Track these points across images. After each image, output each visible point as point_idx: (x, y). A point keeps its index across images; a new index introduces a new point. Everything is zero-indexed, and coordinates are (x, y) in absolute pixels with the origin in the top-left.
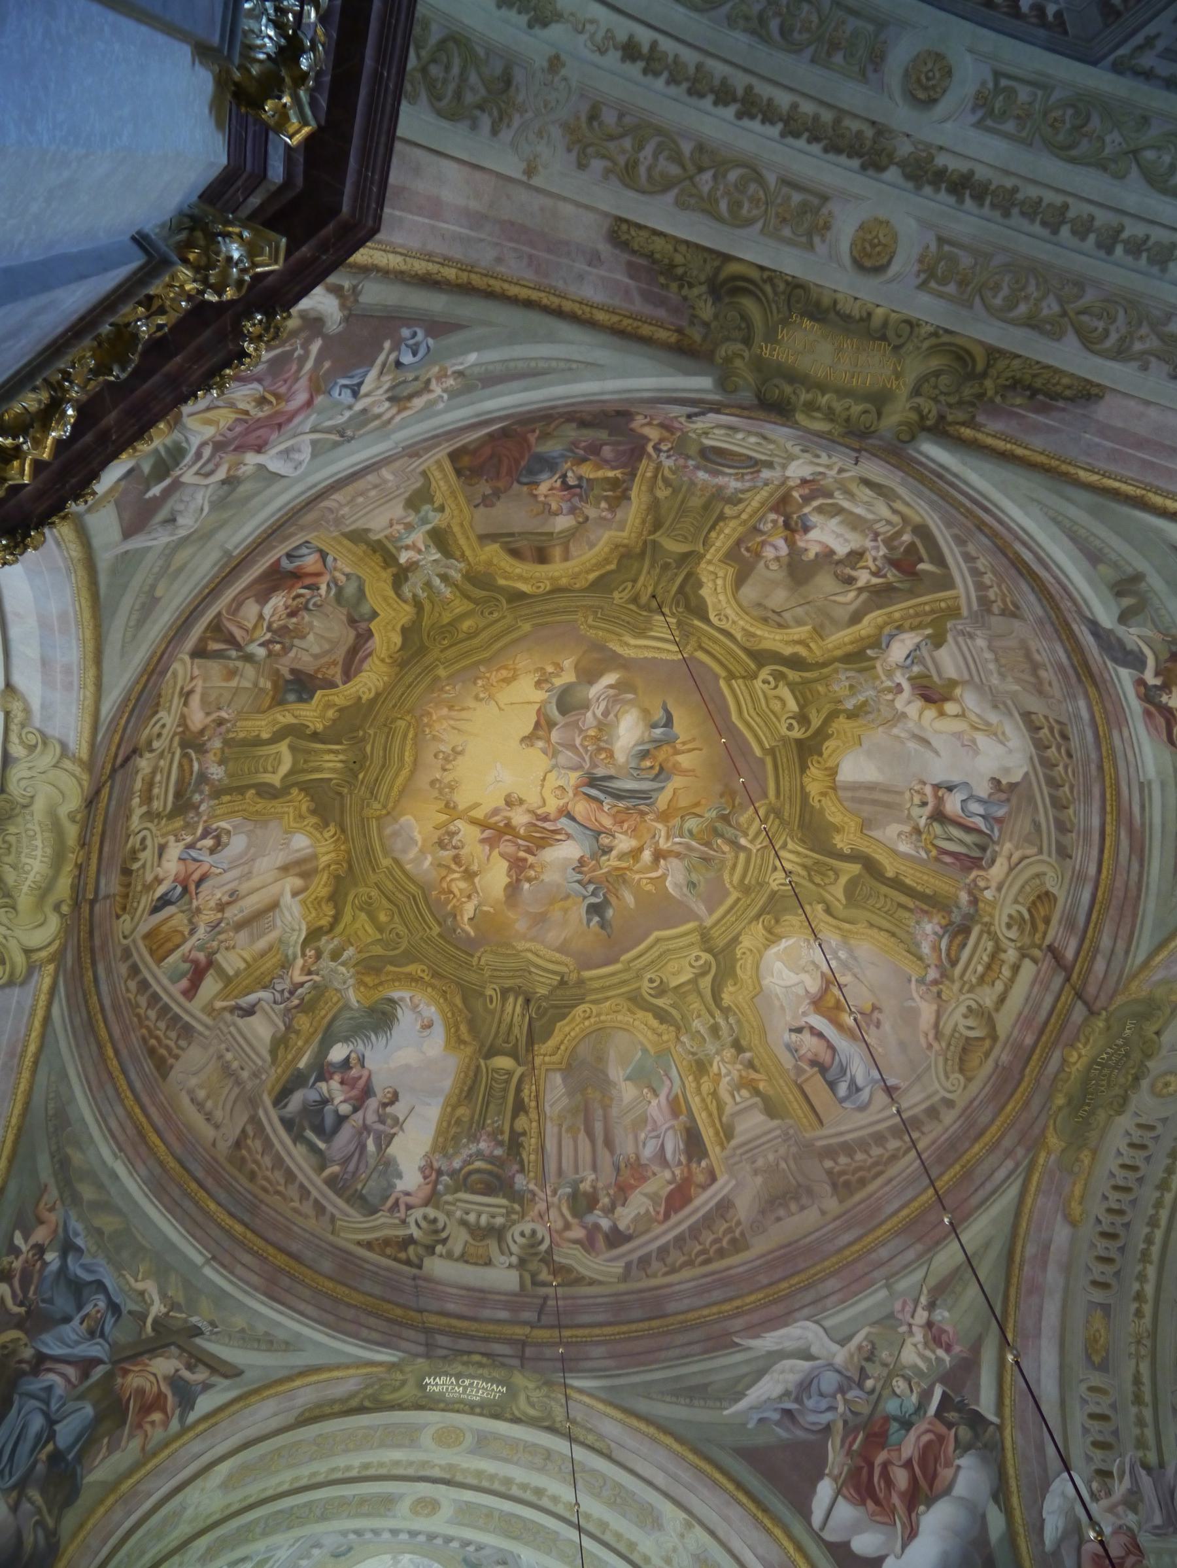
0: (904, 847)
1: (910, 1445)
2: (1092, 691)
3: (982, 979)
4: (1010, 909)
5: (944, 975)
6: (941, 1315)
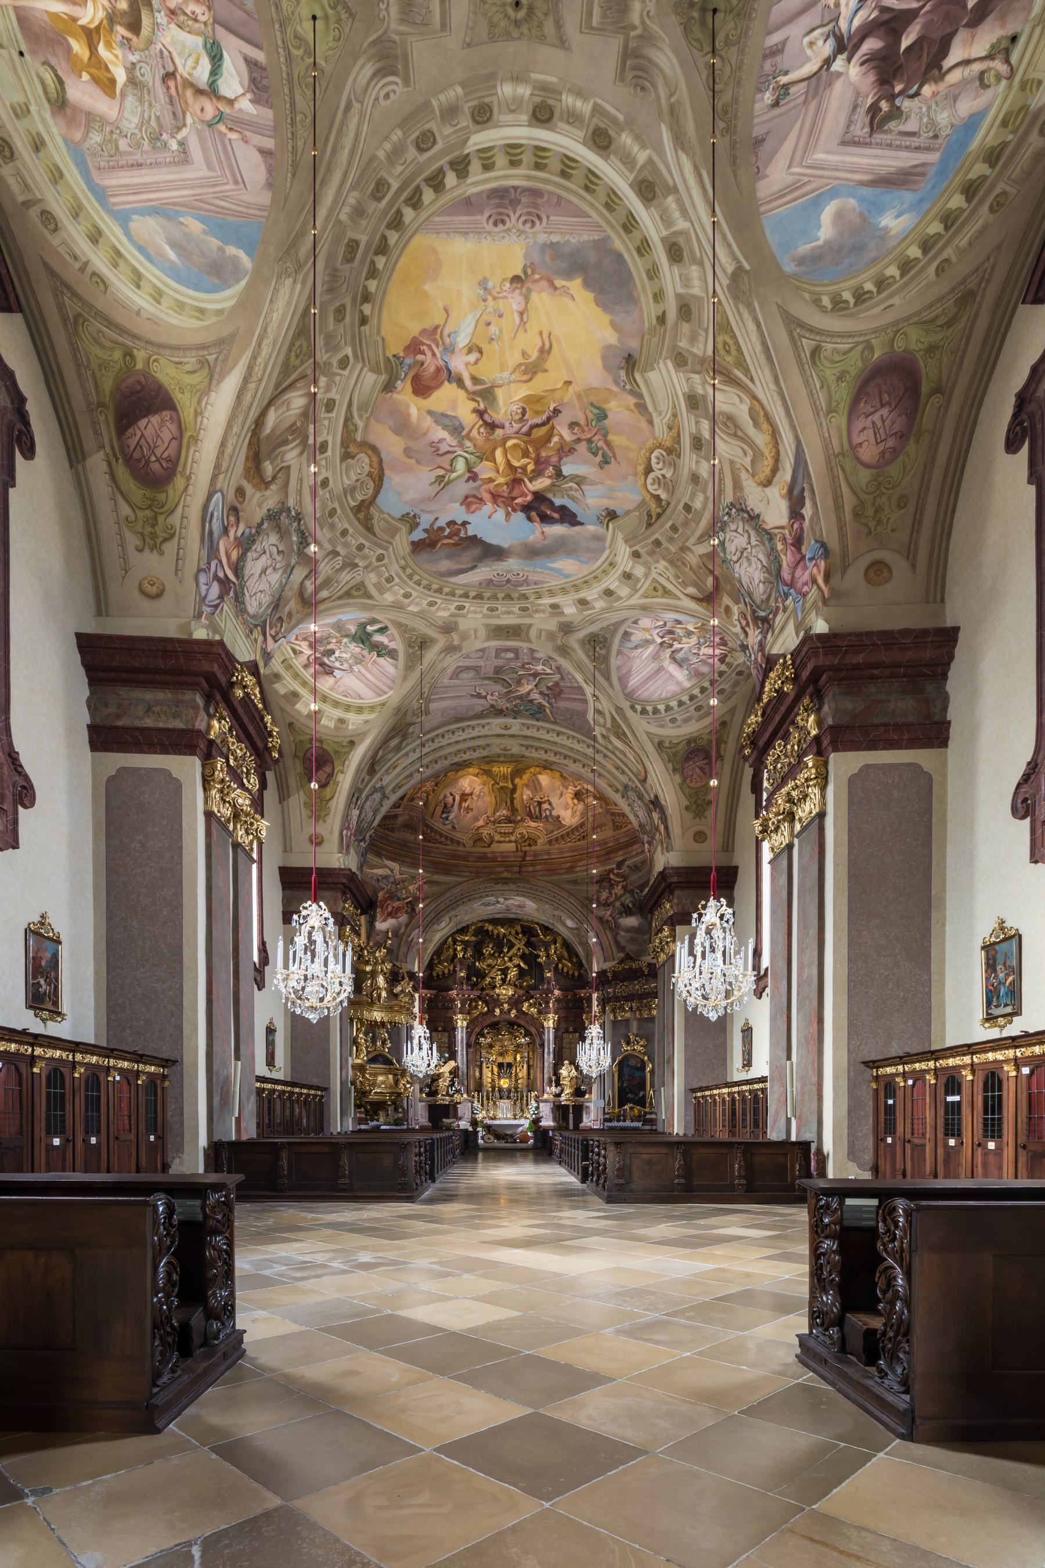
0: (525, 797)
1: (396, 904)
2: (604, 852)
3: (500, 833)
4: (525, 832)
5: (494, 822)
6: (426, 887)
